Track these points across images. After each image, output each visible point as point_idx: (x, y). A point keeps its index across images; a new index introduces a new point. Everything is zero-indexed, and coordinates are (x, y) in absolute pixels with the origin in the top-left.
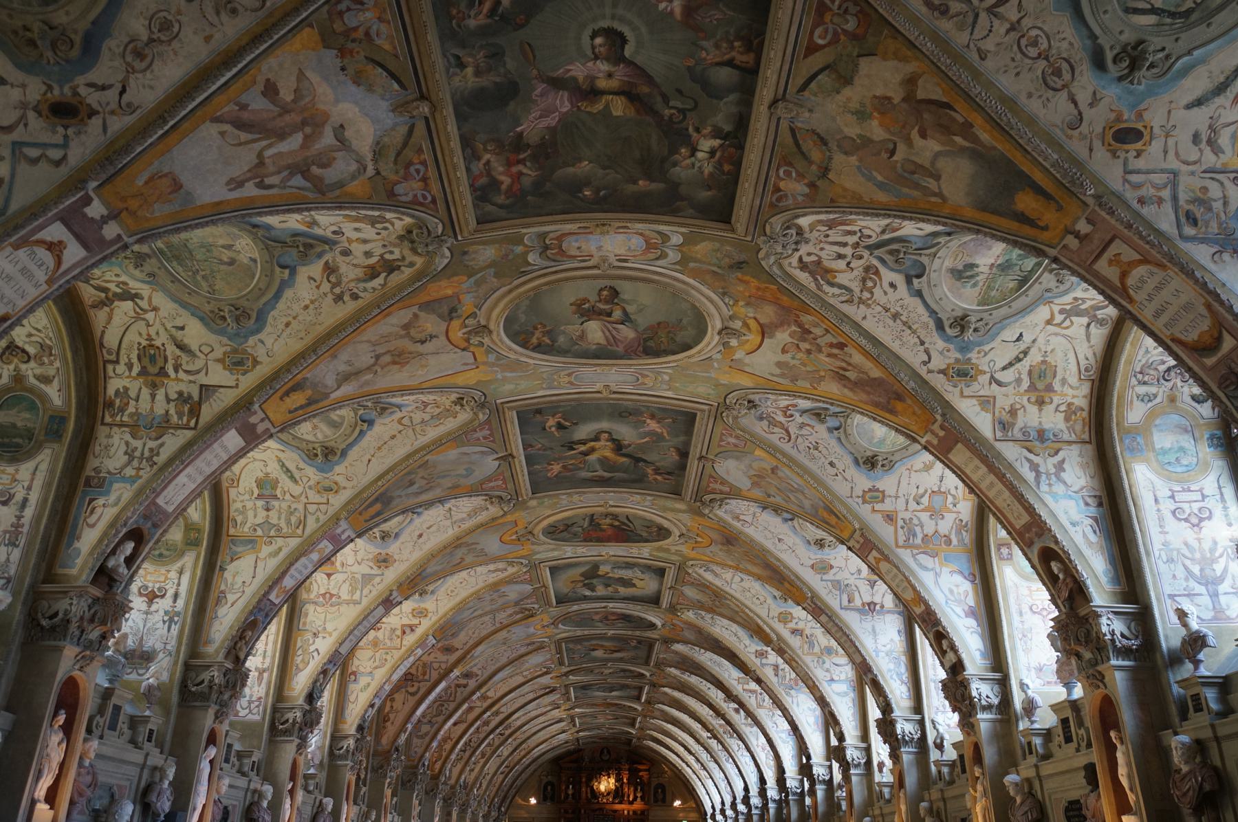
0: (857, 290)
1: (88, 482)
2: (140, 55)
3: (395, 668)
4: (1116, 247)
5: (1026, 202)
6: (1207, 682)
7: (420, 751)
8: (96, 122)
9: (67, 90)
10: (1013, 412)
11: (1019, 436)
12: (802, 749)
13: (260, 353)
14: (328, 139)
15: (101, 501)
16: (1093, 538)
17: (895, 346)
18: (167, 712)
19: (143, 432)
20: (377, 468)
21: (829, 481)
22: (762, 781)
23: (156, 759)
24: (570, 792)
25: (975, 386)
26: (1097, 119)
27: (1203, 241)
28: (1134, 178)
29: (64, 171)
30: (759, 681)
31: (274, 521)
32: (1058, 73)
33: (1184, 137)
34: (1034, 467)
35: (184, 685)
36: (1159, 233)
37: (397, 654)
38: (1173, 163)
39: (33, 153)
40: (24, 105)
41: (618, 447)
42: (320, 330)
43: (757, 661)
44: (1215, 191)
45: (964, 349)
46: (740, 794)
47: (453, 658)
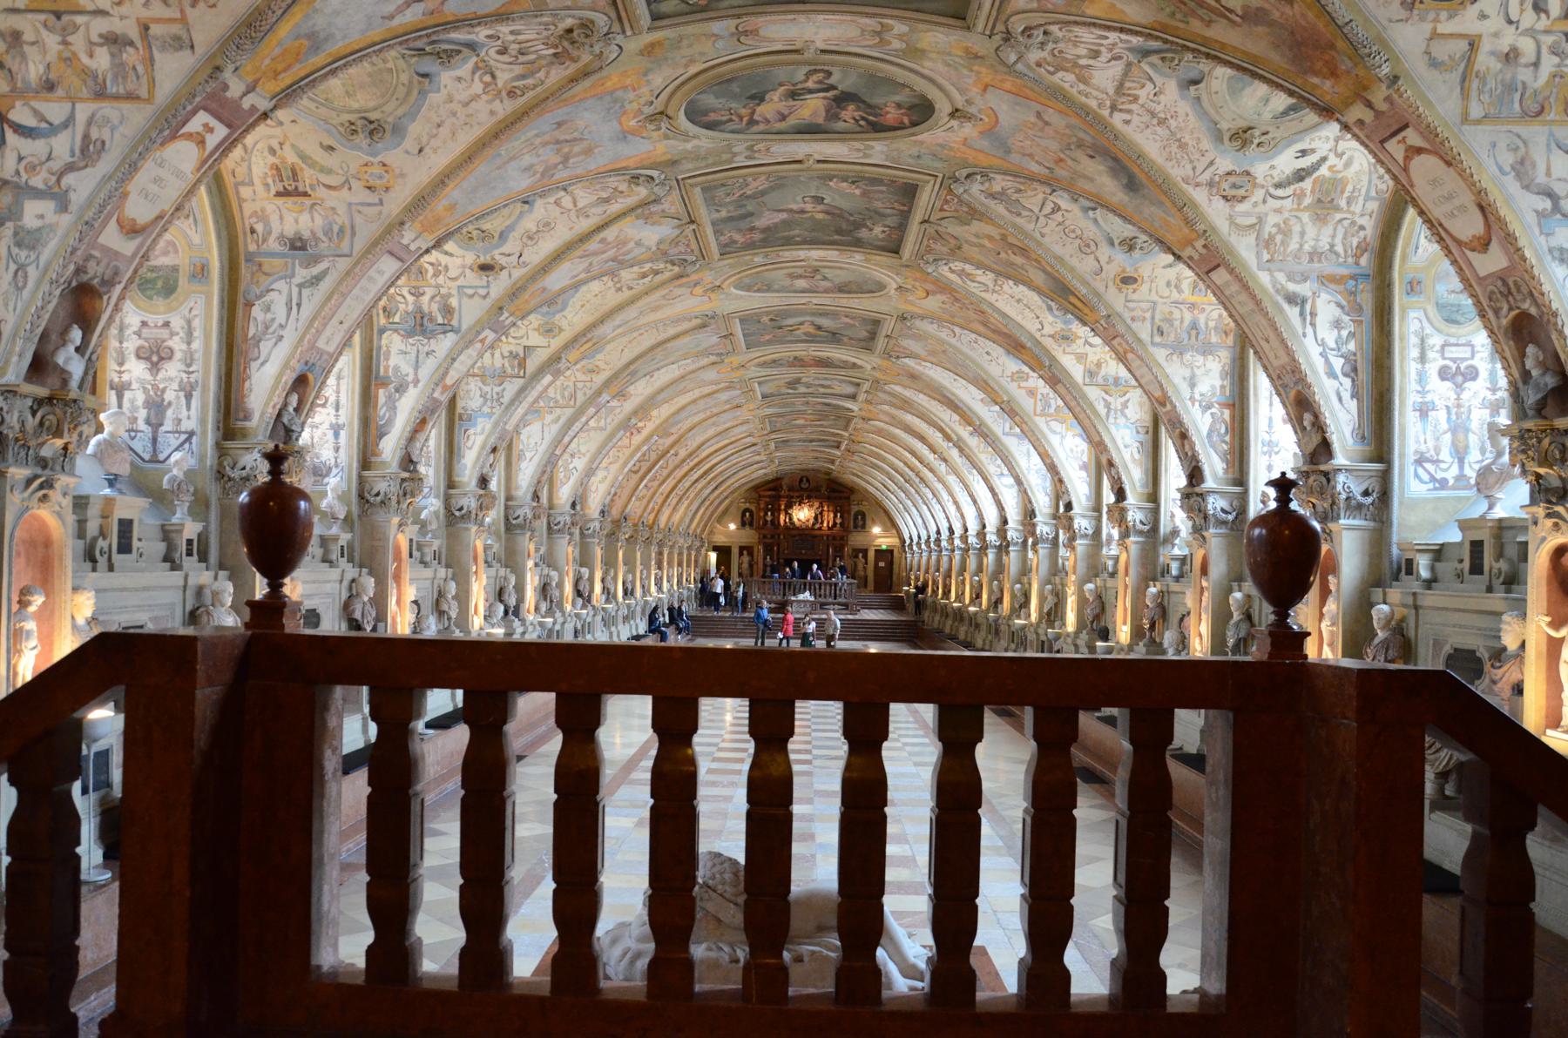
0: (991, 286)
1: (461, 419)
2: (530, 238)
3: (625, 464)
4: (1118, 340)
5: (1073, 299)
6: (1174, 559)
7: (639, 512)
8: (505, 273)
9: (488, 257)
10: (1099, 365)
11: (1100, 380)
12: (980, 516)
13: (564, 324)
14: (632, 245)
15: (471, 431)
16: (1137, 456)
17: (1019, 319)
18: (499, 537)
19: (489, 380)
20: (629, 355)
21: (986, 365)
22: (951, 531)
23: (502, 572)
24: (769, 518)
25: (1074, 346)
26: (1111, 270)
27: (1164, 346)
28: (1131, 305)
29: (489, 301)
30: (945, 460)
31: (552, 395)
32: (1088, 246)
33: (1162, 283)
34: (1108, 406)
35: (507, 518)
36: (1139, 340)
37: (628, 452)
38: (1155, 298)
39: (470, 292)
40: (464, 267)
41: (819, 328)
42: (606, 308)
43: (945, 444)
44: (1177, 314)
45: (1066, 323)
46: (933, 537)
47: (669, 441)
